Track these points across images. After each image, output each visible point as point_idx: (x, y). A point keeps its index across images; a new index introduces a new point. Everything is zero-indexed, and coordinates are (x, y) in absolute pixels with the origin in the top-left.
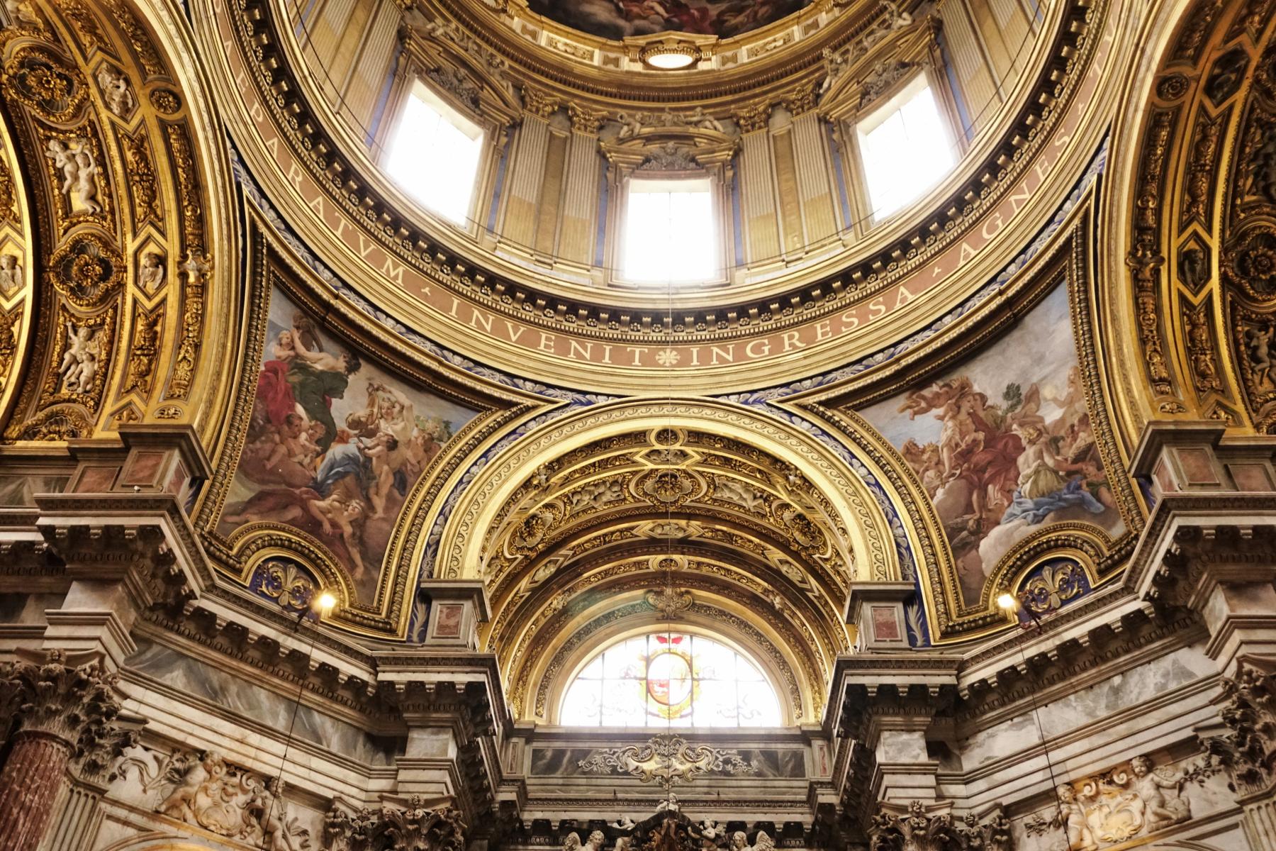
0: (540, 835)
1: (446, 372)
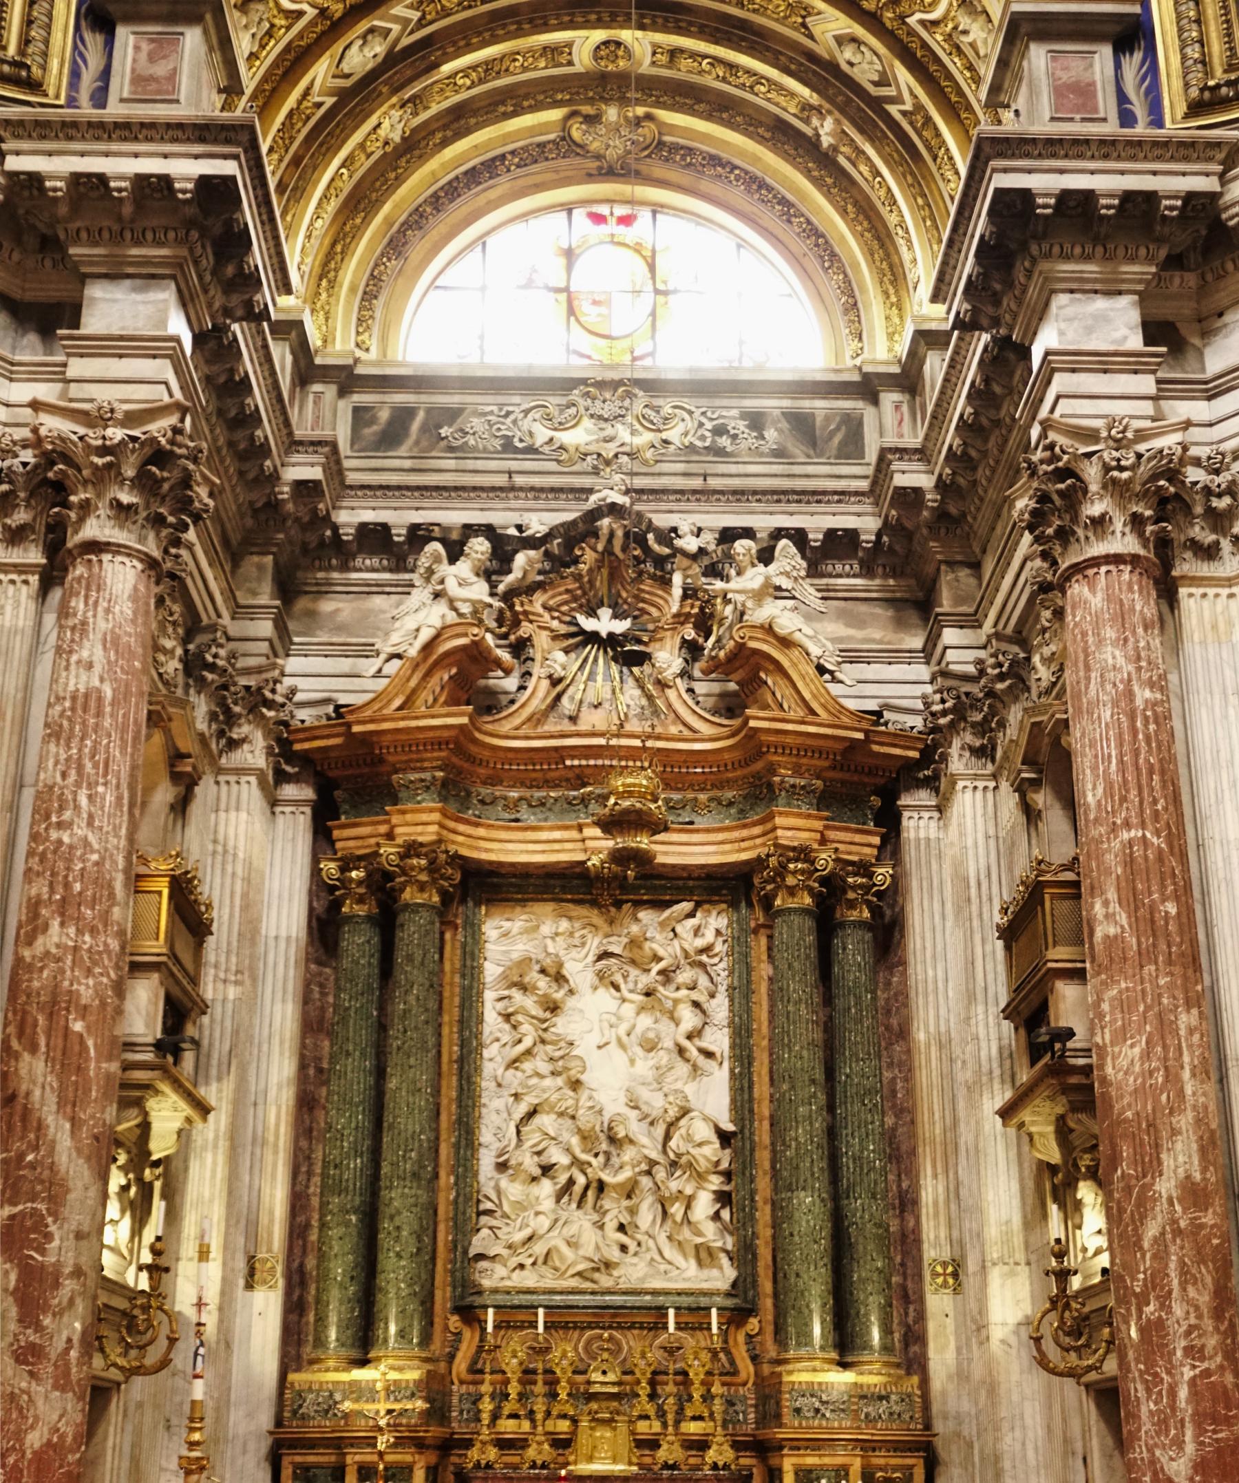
0: (372, 553)
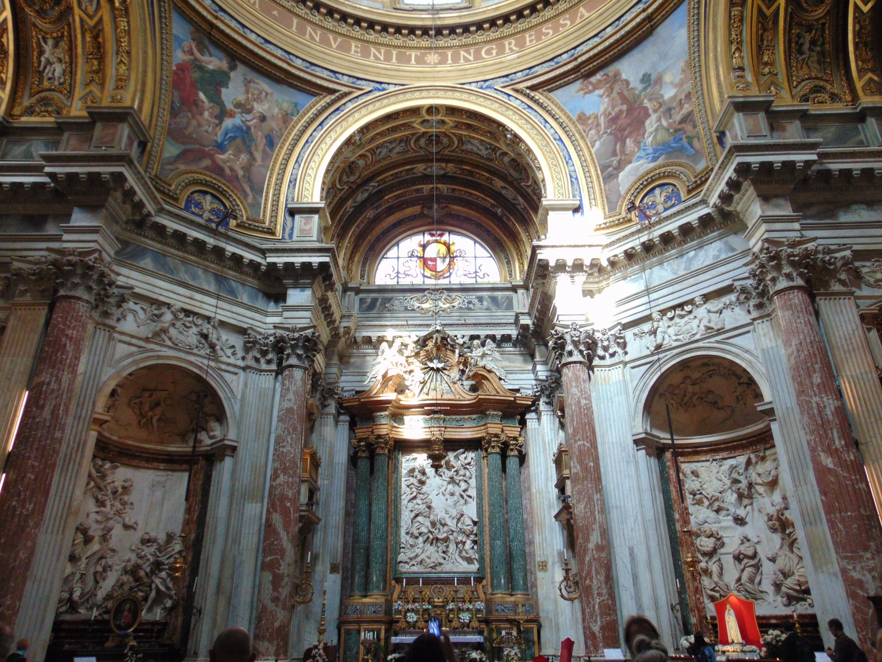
1: (293, 71)
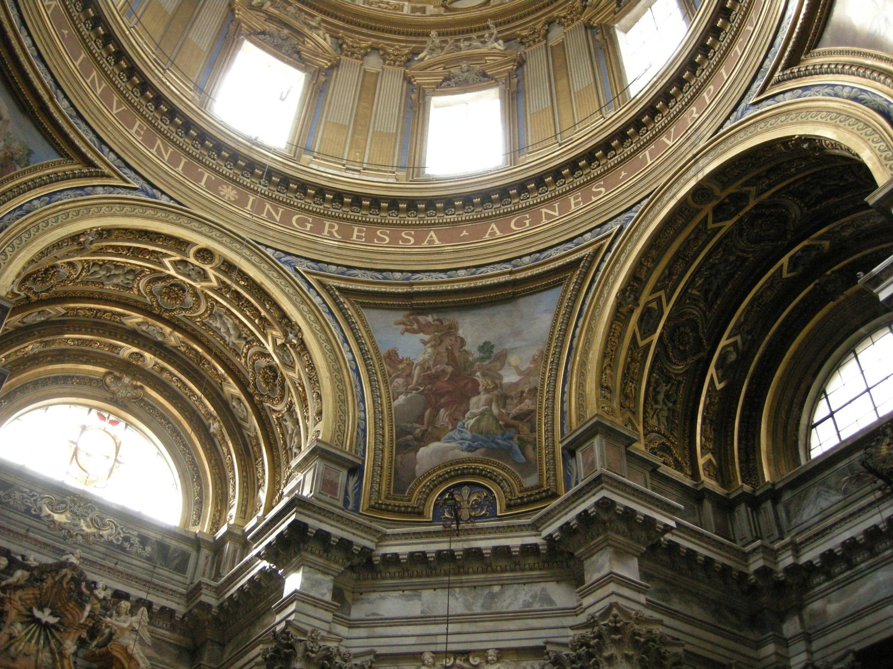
1: (52, 109)
